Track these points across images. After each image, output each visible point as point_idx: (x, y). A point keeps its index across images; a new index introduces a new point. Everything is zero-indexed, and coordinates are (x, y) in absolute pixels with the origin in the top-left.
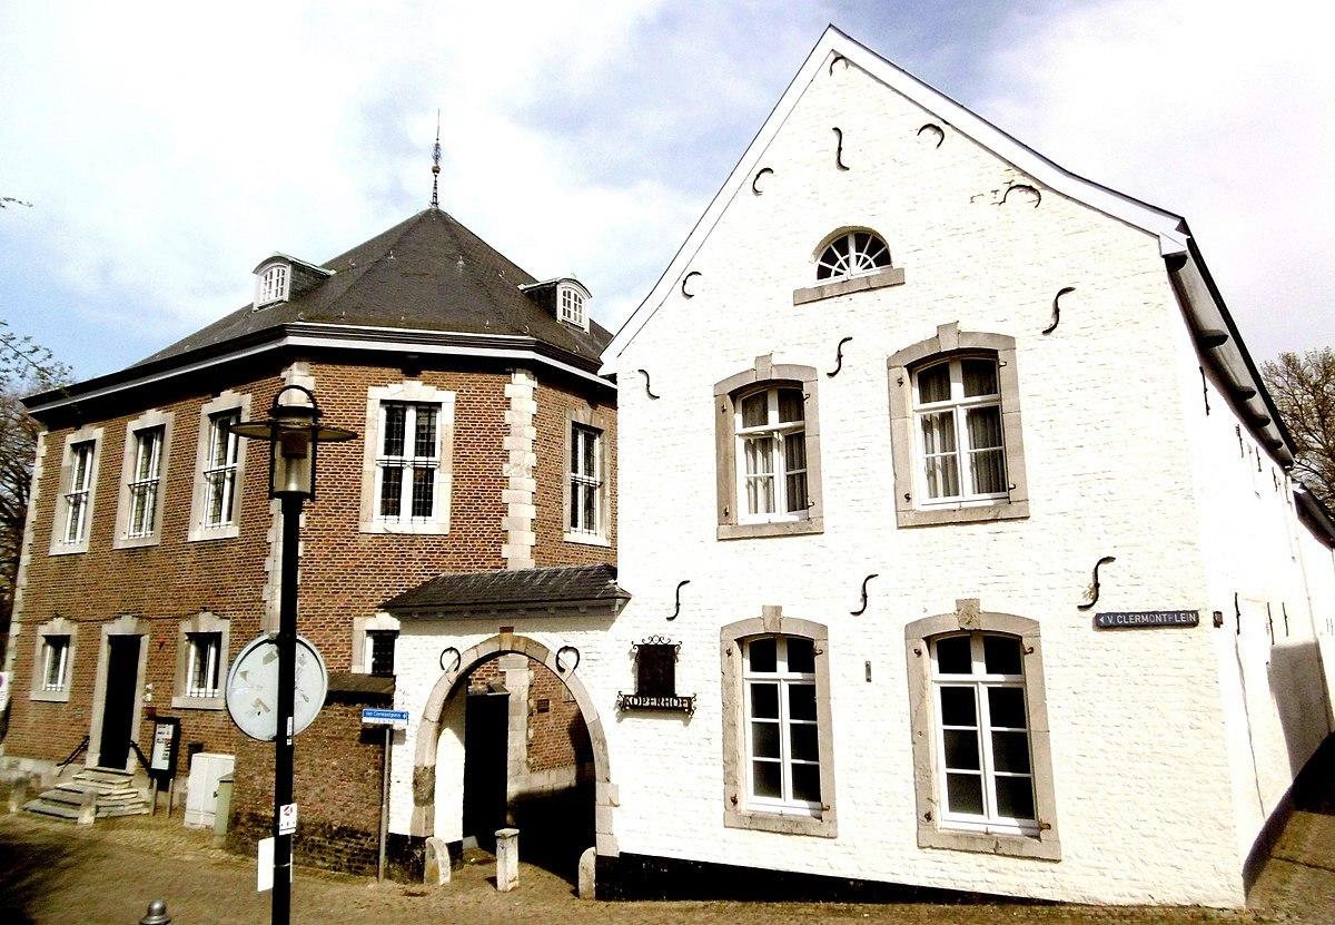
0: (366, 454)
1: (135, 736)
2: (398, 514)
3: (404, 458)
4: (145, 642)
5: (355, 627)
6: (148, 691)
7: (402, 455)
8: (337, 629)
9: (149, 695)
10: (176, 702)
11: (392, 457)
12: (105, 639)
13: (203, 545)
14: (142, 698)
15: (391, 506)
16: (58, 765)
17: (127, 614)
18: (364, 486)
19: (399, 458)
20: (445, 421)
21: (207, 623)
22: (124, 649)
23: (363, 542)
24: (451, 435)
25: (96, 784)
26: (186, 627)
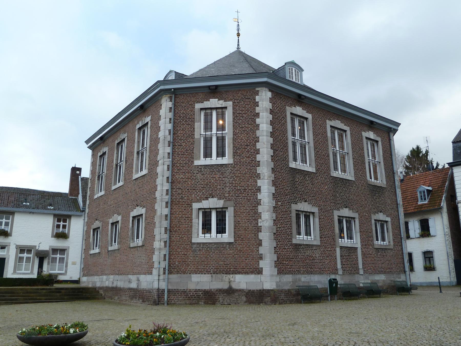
2: (211, 157)
3: (212, 133)
7: (211, 131)
11: (207, 133)
19: (210, 133)
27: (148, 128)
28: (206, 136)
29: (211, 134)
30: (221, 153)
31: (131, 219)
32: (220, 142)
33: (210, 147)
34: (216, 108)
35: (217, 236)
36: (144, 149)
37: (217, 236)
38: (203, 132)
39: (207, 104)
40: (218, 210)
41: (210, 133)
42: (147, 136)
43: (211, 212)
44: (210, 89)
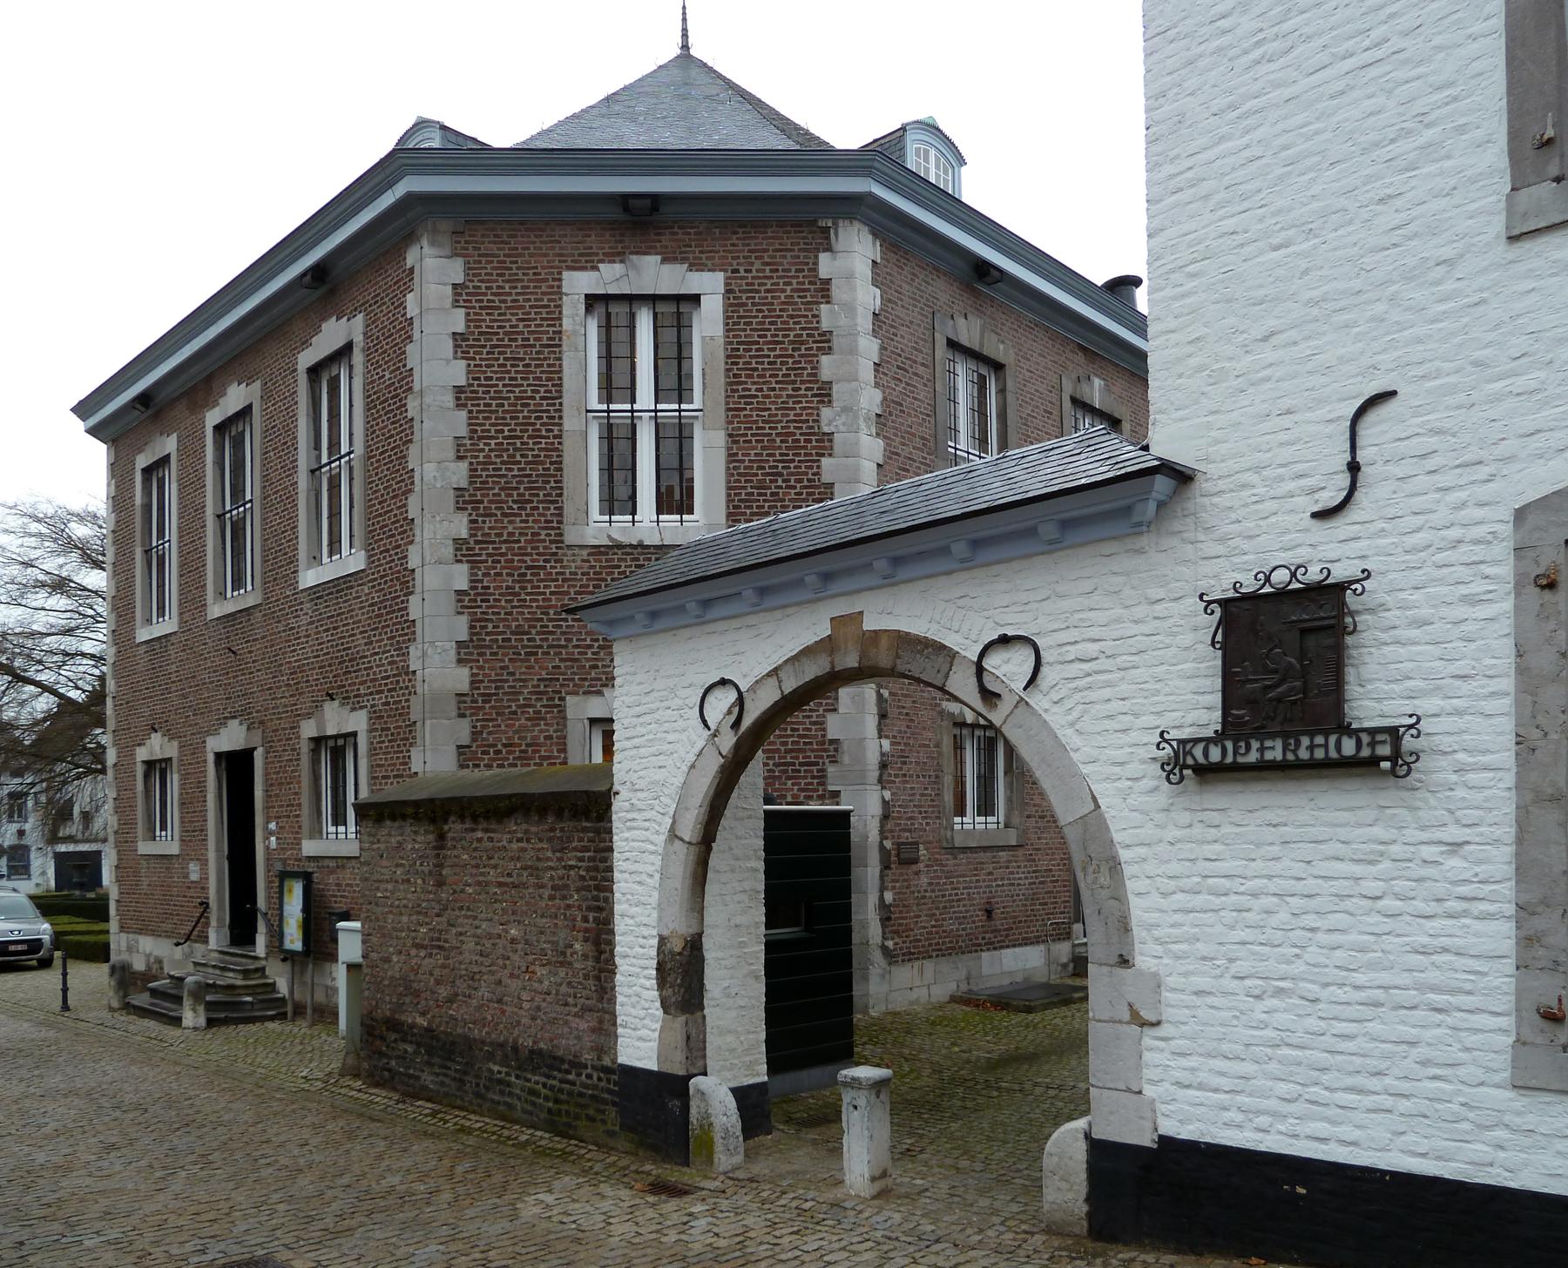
0: (567, 399)
1: (261, 902)
2: (634, 513)
3: (636, 407)
4: (258, 755)
5: (570, 714)
6: (271, 833)
7: (633, 401)
8: (537, 718)
9: (273, 839)
10: (310, 848)
11: (612, 407)
12: (211, 758)
13: (317, 592)
14: (265, 842)
15: (619, 499)
16: (177, 944)
17: (235, 717)
18: (567, 459)
19: (628, 407)
20: (708, 324)
21: (337, 719)
22: (237, 766)
23: (573, 564)
24: (721, 355)
25: (218, 972)
26: (309, 729)
27: (351, 367)
28: (608, 417)
29: (632, 411)
30: (674, 498)
31: (305, 748)
33: (630, 467)
34: (653, 299)
36: (339, 459)
38: (594, 404)
39: (609, 277)
41: (628, 407)
42: (351, 406)
44: (626, 209)
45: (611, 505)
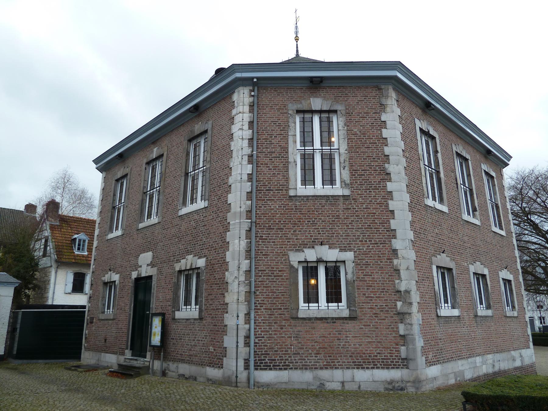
7: (313, 146)
11: (306, 148)
32: (327, 161)
35: (328, 306)
37: (328, 306)
38: (299, 147)
40: (329, 264)
43: (316, 268)
45: (304, 182)
